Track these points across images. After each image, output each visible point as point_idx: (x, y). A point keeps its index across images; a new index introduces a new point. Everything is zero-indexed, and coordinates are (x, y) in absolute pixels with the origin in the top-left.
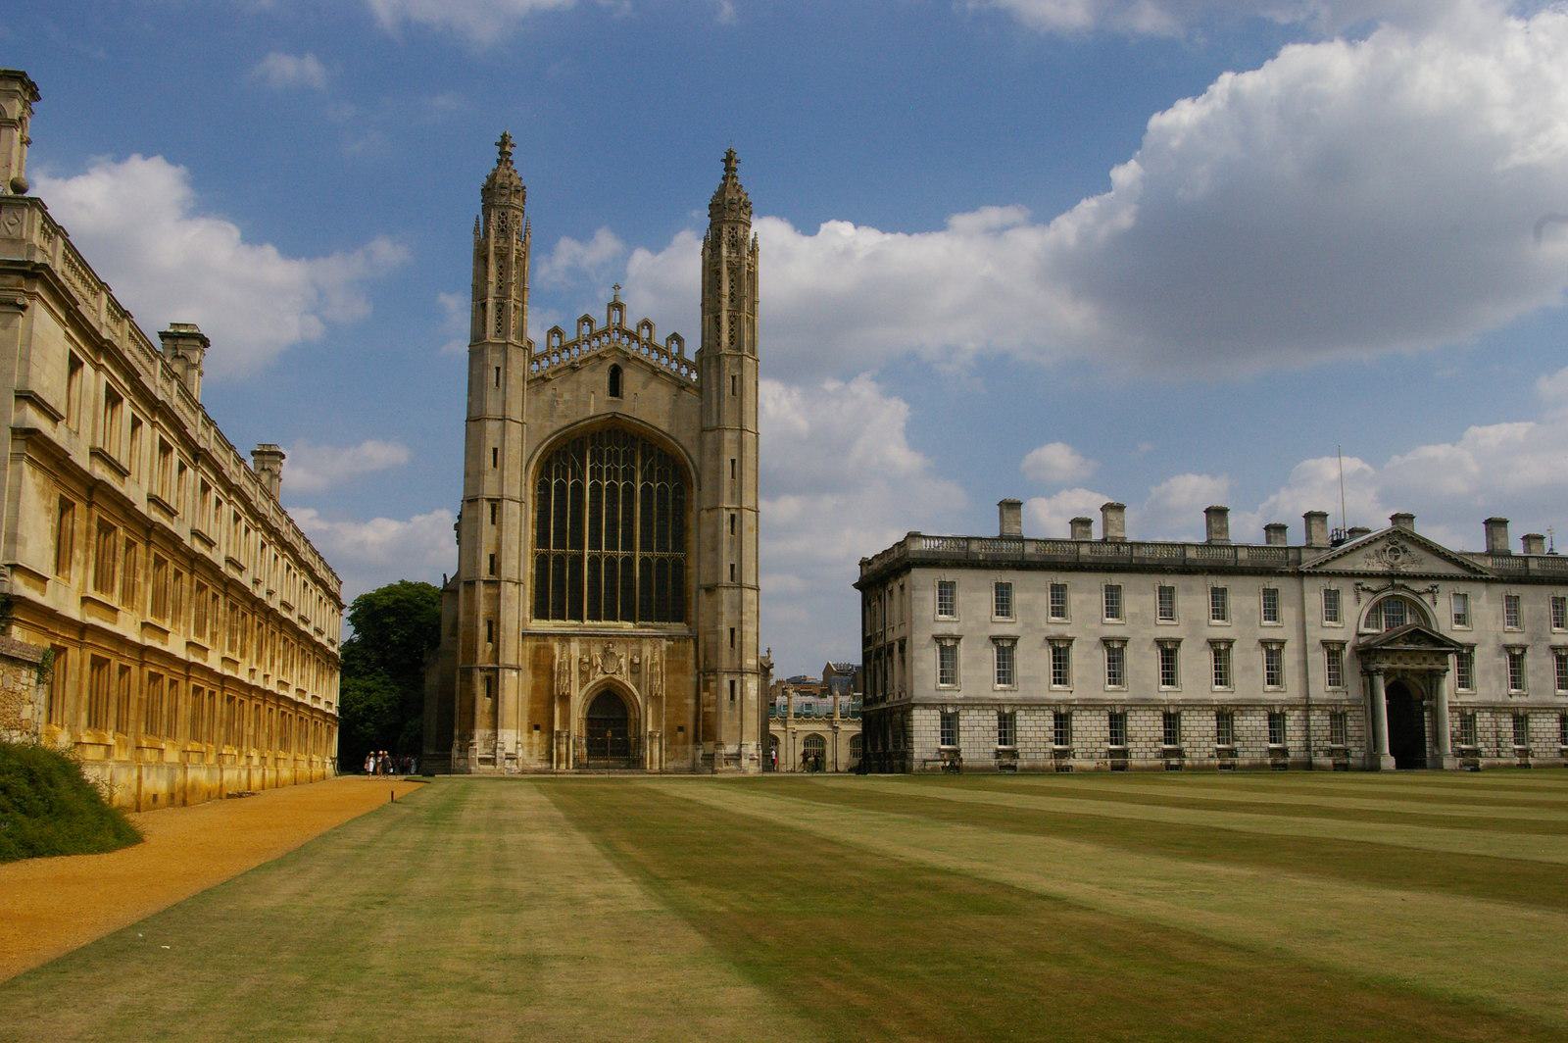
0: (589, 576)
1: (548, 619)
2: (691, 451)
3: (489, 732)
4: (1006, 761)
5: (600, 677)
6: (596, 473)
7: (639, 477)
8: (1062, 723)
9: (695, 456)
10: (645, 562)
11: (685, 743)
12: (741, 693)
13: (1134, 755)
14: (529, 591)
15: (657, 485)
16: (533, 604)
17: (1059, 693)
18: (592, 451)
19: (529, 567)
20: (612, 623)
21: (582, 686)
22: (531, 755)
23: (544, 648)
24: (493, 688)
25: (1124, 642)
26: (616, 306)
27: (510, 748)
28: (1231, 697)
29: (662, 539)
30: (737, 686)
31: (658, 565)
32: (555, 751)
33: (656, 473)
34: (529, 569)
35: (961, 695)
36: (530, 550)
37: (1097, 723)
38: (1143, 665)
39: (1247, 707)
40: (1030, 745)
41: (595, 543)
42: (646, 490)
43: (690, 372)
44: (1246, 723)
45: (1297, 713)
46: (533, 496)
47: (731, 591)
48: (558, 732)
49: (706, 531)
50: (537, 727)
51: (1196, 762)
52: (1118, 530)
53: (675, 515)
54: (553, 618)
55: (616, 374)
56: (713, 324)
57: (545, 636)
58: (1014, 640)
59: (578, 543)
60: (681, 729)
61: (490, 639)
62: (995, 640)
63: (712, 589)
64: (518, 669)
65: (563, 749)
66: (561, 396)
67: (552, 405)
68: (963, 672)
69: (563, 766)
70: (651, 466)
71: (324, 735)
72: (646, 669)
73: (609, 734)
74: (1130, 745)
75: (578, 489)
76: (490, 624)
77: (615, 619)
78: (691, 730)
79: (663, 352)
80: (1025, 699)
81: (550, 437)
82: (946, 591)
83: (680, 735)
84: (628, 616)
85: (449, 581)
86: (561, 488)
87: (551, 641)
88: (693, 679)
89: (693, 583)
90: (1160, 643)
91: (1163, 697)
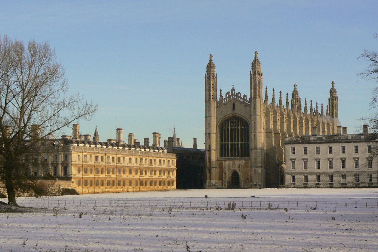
3: (209, 180)
4: (305, 186)
6: (231, 126)
7: (240, 126)
8: (319, 178)
9: (249, 121)
10: (241, 144)
11: (248, 182)
13: (334, 184)
17: (318, 171)
18: (231, 121)
20: (235, 157)
25: (333, 159)
26: (233, 90)
27: (214, 184)
28: (359, 171)
32: (223, 184)
34: (219, 147)
35: (296, 171)
36: (218, 143)
37: (326, 177)
38: (337, 165)
39: (362, 173)
40: (311, 182)
41: (231, 141)
42: (241, 129)
43: (248, 103)
44: (362, 177)
45: (375, 174)
46: (219, 132)
48: (224, 180)
50: (220, 179)
51: (349, 186)
52: (339, 132)
54: (224, 157)
55: (234, 105)
57: (221, 160)
58: (307, 160)
59: (228, 141)
60: (248, 179)
62: (303, 159)
63: (251, 150)
64: (216, 168)
65: (225, 183)
66: (223, 110)
67: (221, 112)
68: (296, 167)
69: (225, 187)
70: (242, 124)
72: (240, 166)
73: (234, 180)
74: (334, 182)
75: (228, 129)
77: (236, 156)
78: (250, 179)
80: (310, 172)
81: (221, 119)
82: (293, 149)
83: (247, 180)
84: (238, 156)
86: (225, 130)
88: (250, 169)
89: (250, 149)
90: (341, 159)
91: (342, 171)
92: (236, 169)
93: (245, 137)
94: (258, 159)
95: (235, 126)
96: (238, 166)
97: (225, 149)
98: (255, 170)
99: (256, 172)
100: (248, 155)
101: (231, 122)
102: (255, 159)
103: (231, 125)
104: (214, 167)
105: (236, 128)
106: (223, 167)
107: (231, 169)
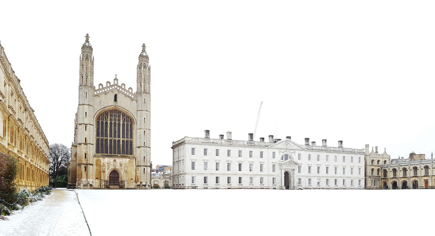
0: (109, 143)
1: (99, 153)
2: (134, 116)
5: (113, 167)
7: (121, 121)
10: (123, 141)
12: (146, 171)
14: (95, 146)
15: (126, 123)
16: (96, 150)
19: (95, 141)
20: (115, 155)
21: (108, 169)
22: (96, 185)
23: (99, 160)
24: (86, 169)
29: (127, 135)
30: (145, 170)
31: (126, 142)
33: (126, 120)
34: (94, 142)
36: (95, 137)
41: (111, 136)
42: (123, 124)
47: (144, 148)
49: (138, 134)
53: (130, 130)
54: (101, 153)
56: (140, 86)
60: (132, 179)
61: (85, 158)
64: (92, 165)
70: (124, 118)
71: (47, 179)
75: (106, 123)
76: (85, 154)
77: (116, 154)
78: (134, 179)
79: (128, 91)
84: (119, 153)
85: (73, 144)
86: (102, 123)
87: (100, 158)
88: (135, 168)
89: (134, 146)
92: (118, 167)
93: (127, 133)
94: (148, 157)
95: (115, 120)
96: (120, 164)
97: (102, 145)
98: (144, 169)
99: (145, 172)
100: (131, 153)
101: (111, 116)
102: (144, 157)
103: (110, 118)
104: (91, 164)
105: (117, 122)
106: (101, 165)
107: (112, 167)
